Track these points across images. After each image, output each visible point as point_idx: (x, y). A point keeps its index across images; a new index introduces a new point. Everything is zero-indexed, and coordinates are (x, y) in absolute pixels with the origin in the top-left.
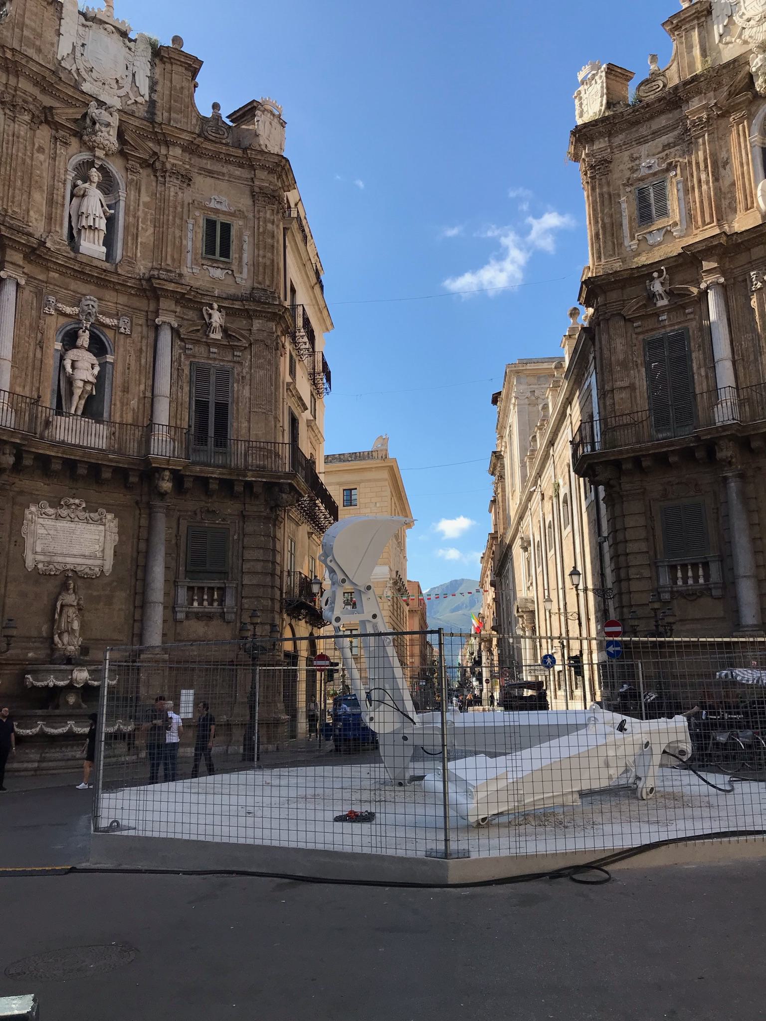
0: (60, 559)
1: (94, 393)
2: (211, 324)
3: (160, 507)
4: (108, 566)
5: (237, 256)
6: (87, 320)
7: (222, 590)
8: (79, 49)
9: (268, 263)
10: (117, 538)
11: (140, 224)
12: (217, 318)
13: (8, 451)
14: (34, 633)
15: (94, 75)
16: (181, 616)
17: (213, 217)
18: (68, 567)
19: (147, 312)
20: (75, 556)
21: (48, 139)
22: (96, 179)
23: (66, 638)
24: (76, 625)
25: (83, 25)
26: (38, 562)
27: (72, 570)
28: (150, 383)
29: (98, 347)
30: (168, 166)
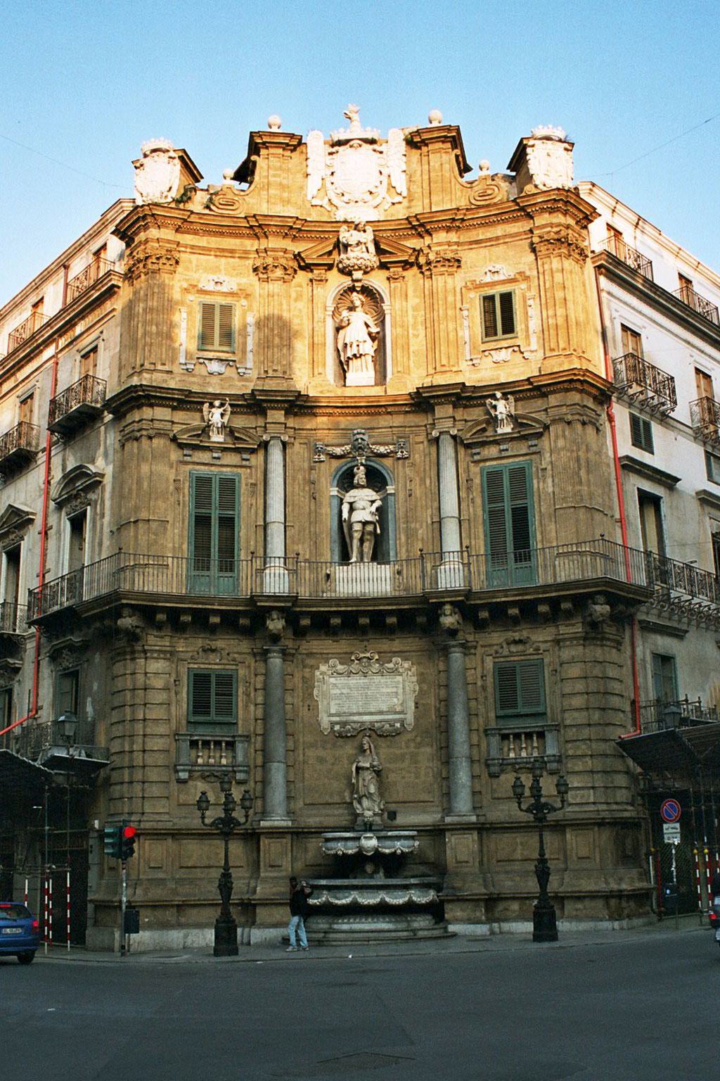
0: (356, 718)
1: (379, 531)
2: (496, 416)
3: (454, 646)
4: (410, 718)
5: (523, 326)
6: (360, 455)
7: (541, 735)
8: (329, 179)
9: (560, 321)
10: (417, 688)
11: (411, 331)
12: (502, 408)
13: (275, 617)
14: (336, 799)
15: (345, 198)
16: (494, 769)
17: (490, 292)
19: (425, 426)
20: (371, 714)
21: (304, 285)
22: (358, 303)
23: (366, 802)
24: (372, 789)
25: (331, 154)
26: (333, 724)
27: (370, 729)
28: (436, 504)
29: (376, 480)
30: (432, 257)
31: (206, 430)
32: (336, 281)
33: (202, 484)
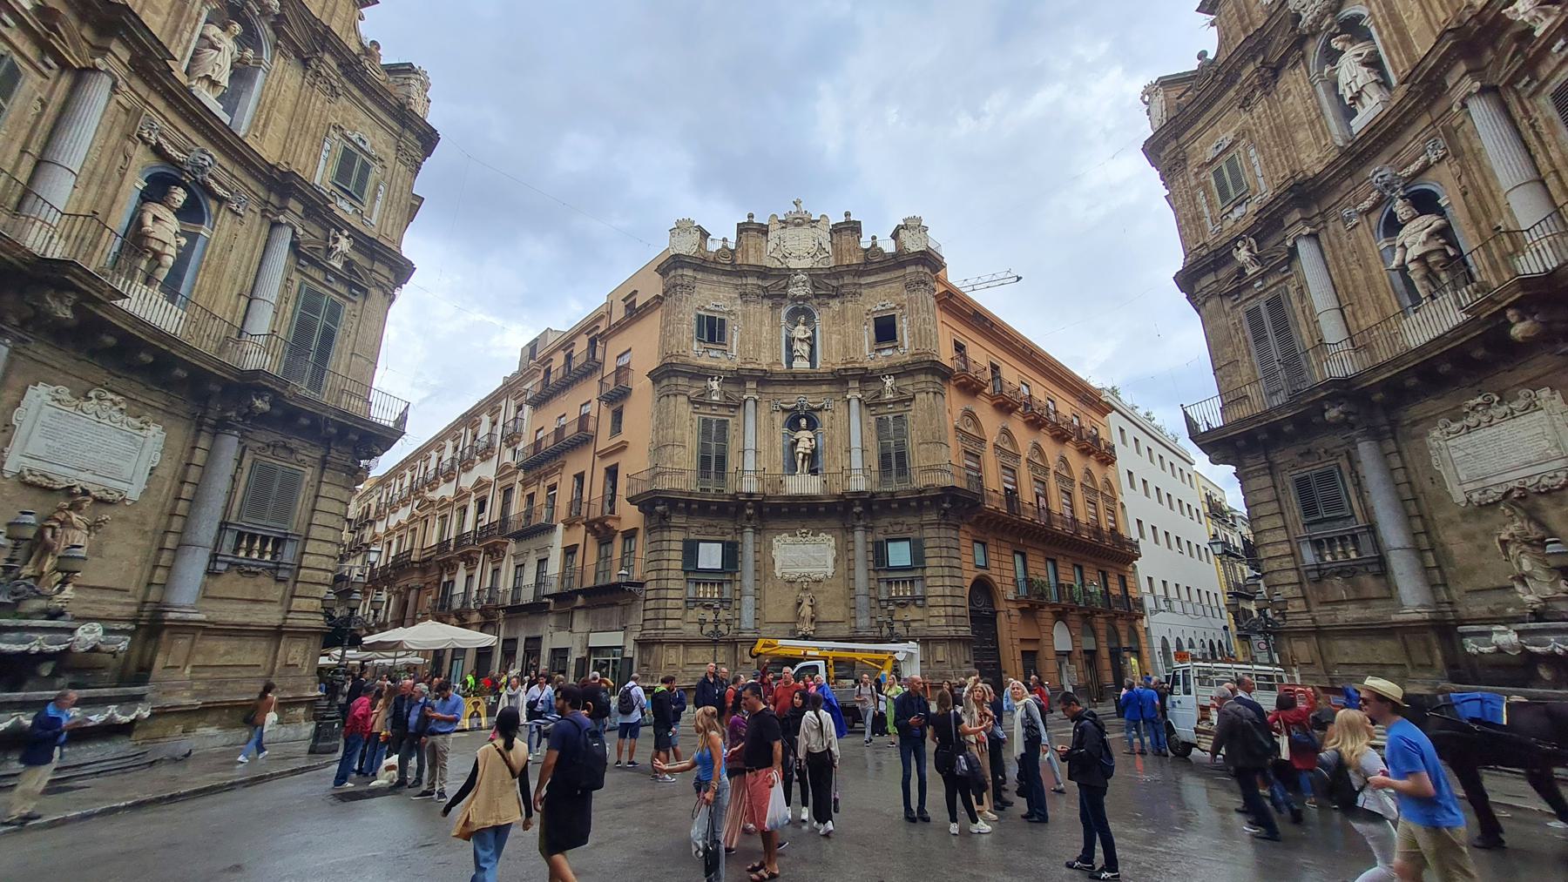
0: (1496, 480)
18: (1511, 485)
22: (1339, 46)
26: (1469, 494)
29: (1425, 202)
31: (1242, 271)
32: (1313, 49)
33: (1253, 315)
